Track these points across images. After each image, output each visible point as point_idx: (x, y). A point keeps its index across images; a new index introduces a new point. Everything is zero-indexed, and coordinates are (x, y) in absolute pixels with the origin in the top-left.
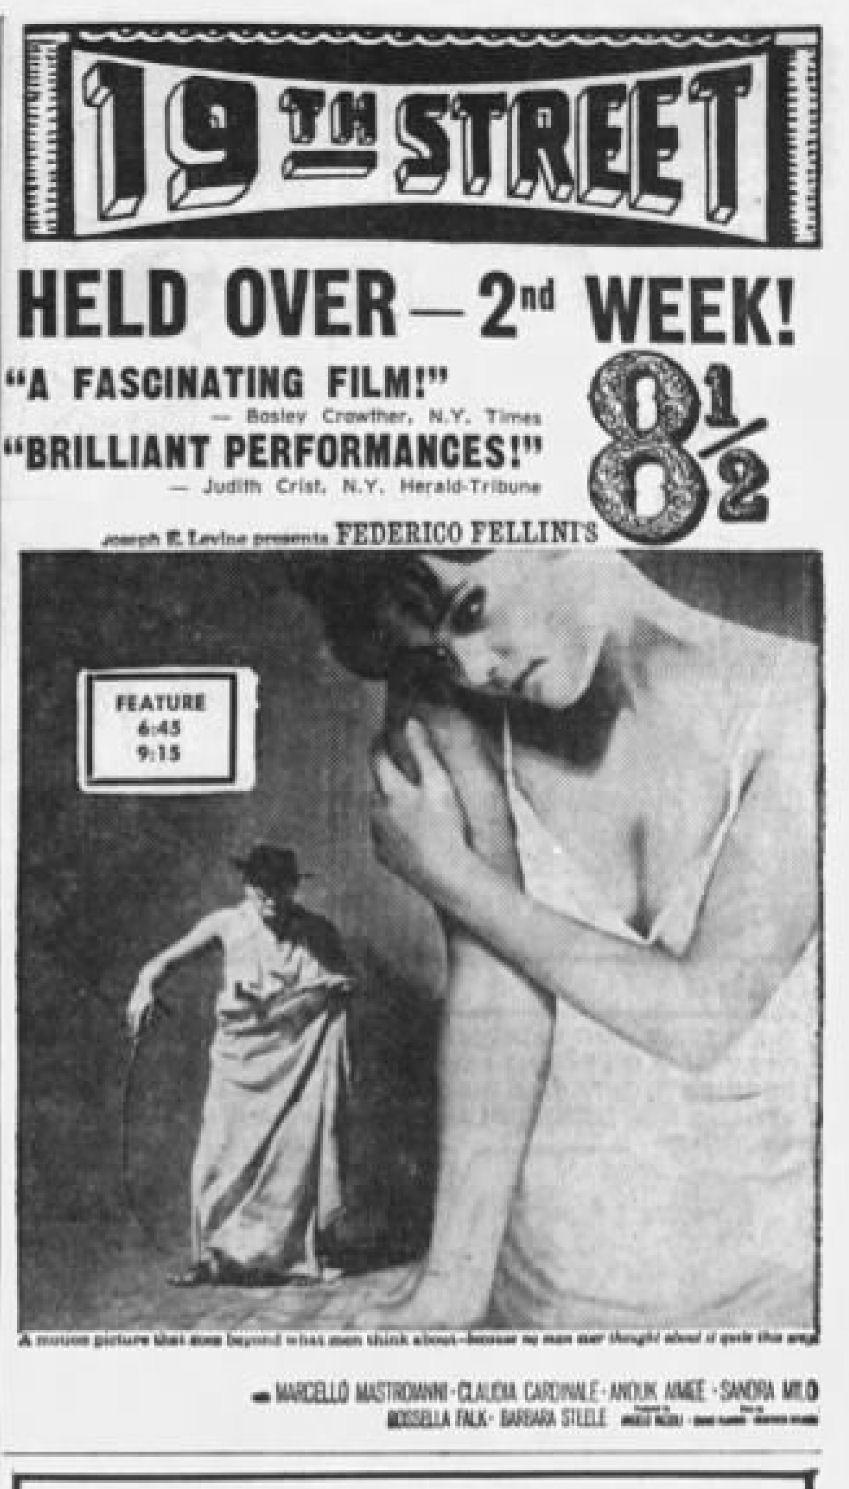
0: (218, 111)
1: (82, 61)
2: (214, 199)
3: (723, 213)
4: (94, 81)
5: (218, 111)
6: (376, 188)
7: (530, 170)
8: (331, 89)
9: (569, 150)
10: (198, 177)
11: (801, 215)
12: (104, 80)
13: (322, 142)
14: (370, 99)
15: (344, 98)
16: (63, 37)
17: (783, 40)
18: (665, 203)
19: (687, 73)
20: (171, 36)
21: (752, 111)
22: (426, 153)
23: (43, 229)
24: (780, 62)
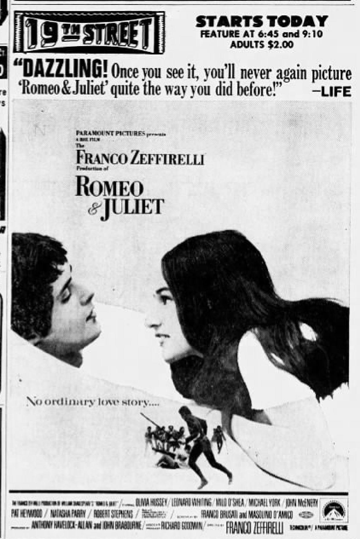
0: (51, 28)
1: (26, 18)
2: (49, 45)
3: (145, 47)
4: (28, 22)
5: (51, 28)
6: (79, 43)
7: (109, 39)
8: (71, 24)
9: (117, 35)
10: (47, 41)
11: (161, 48)
12: (29, 22)
13: (70, 34)
14: (79, 26)
15: (74, 26)
16: (22, 14)
17: (158, 14)
18: (134, 45)
19: (140, 20)
20: (42, 14)
21: (151, 27)
22: (89, 35)
23: (18, 50)
24: (157, 18)
